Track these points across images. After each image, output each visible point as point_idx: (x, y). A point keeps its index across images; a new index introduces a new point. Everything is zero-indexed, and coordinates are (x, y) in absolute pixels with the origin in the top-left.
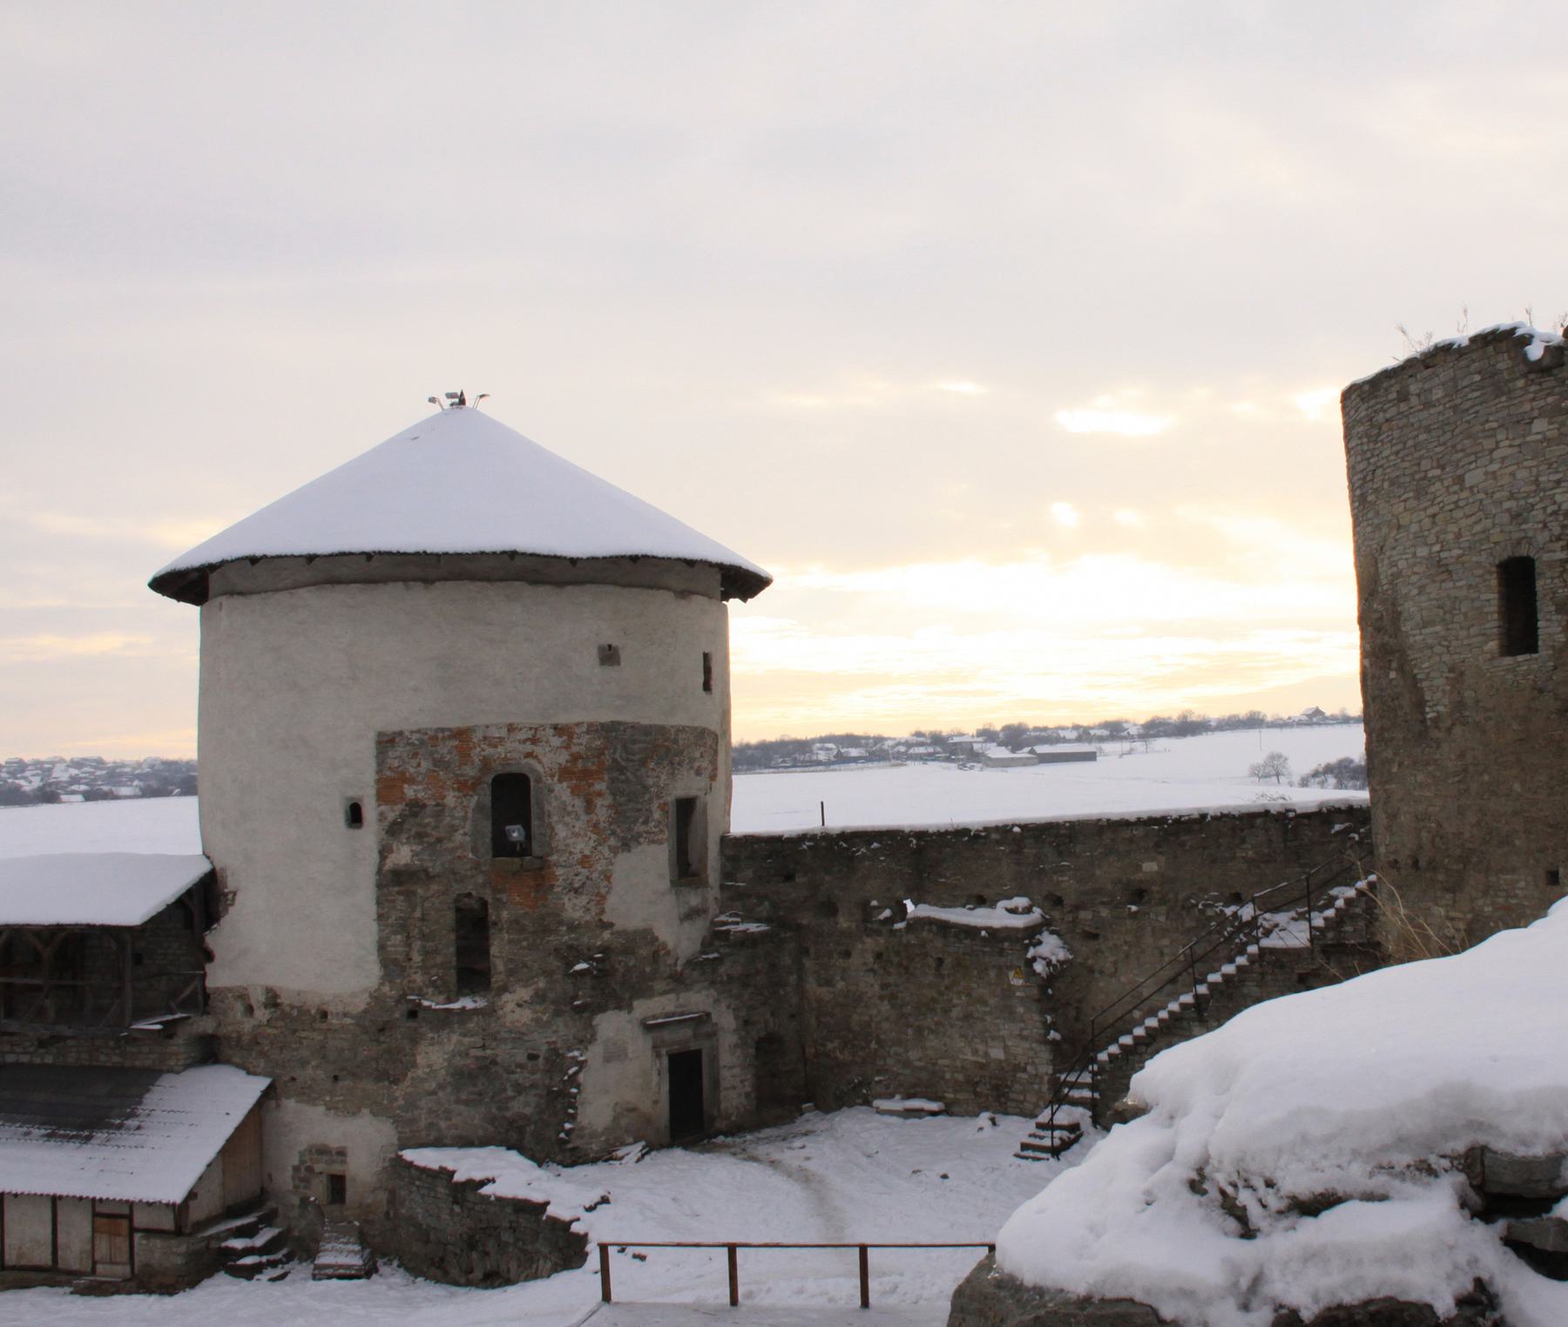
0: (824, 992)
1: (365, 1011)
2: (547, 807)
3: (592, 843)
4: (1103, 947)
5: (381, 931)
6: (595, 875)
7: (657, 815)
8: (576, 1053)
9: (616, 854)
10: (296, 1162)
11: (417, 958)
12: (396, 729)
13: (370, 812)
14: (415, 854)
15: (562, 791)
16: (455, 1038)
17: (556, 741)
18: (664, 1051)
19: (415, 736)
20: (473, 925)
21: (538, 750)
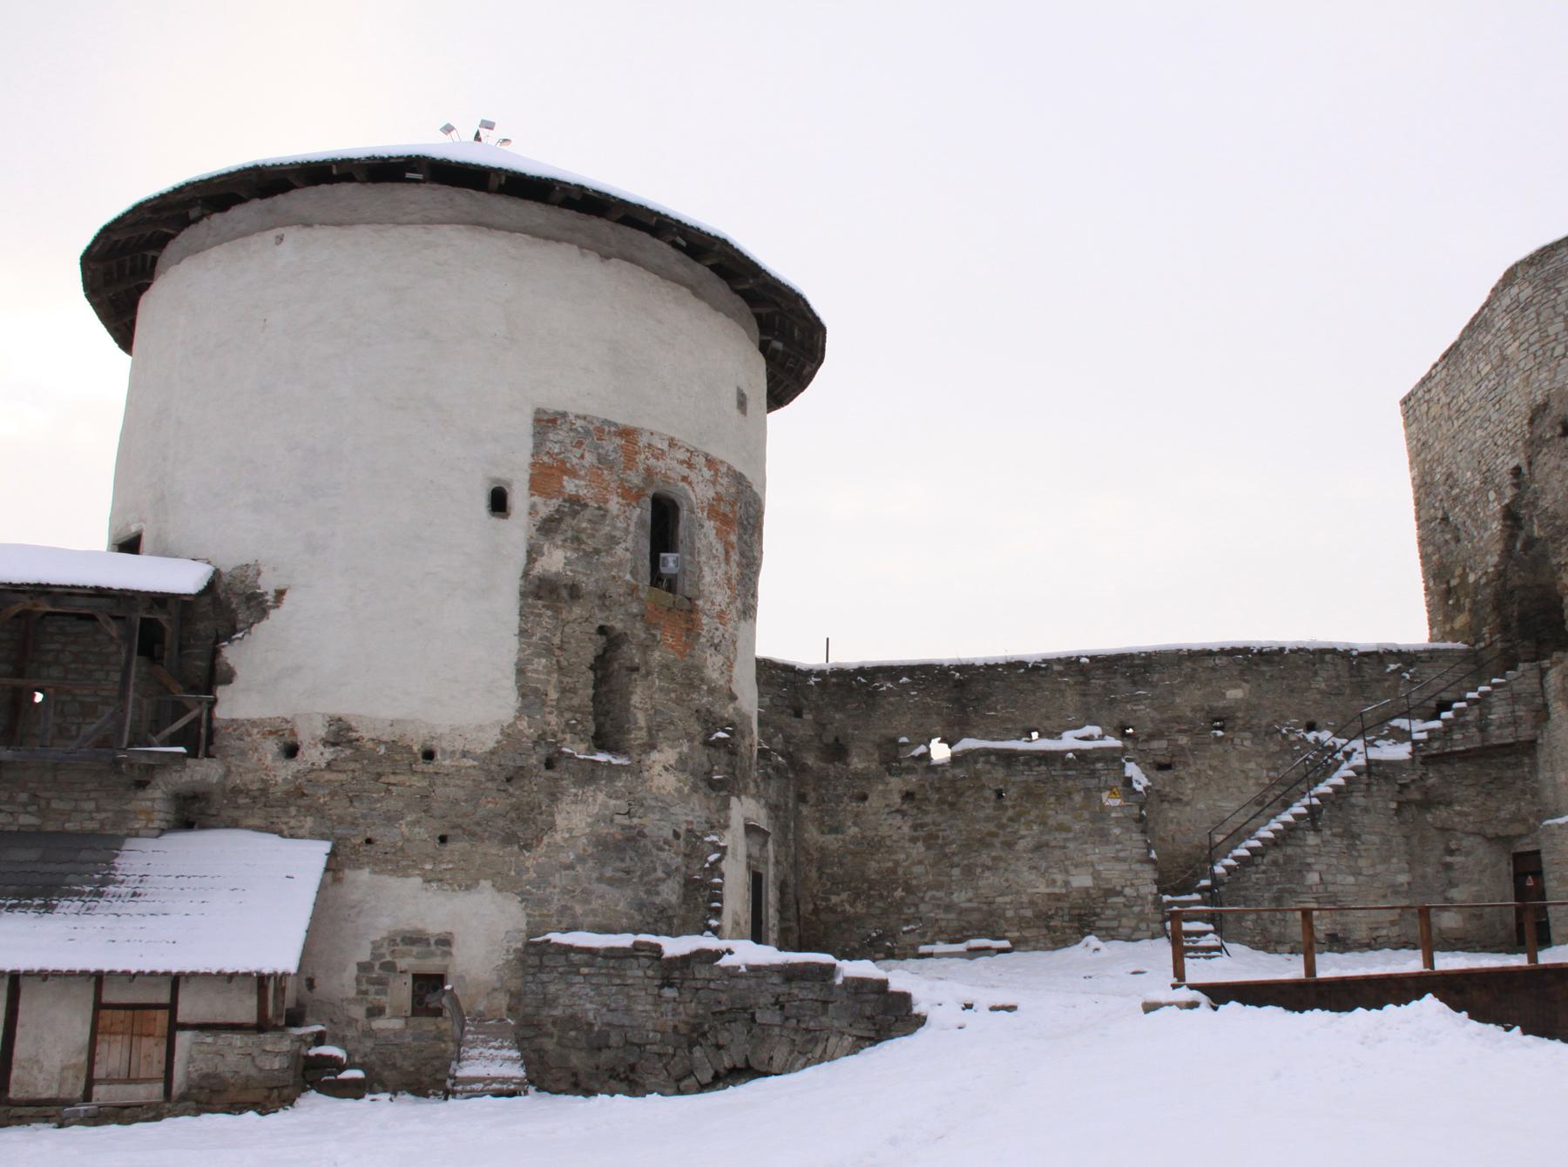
0: (831, 842)
1: (493, 752)
2: (698, 545)
4: (1183, 774)
5: (521, 650)
8: (714, 838)
10: (365, 956)
12: (561, 409)
13: (519, 499)
14: (568, 562)
16: (601, 797)
17: (707, 474)
19: (579, 423)
21: (693, 476)
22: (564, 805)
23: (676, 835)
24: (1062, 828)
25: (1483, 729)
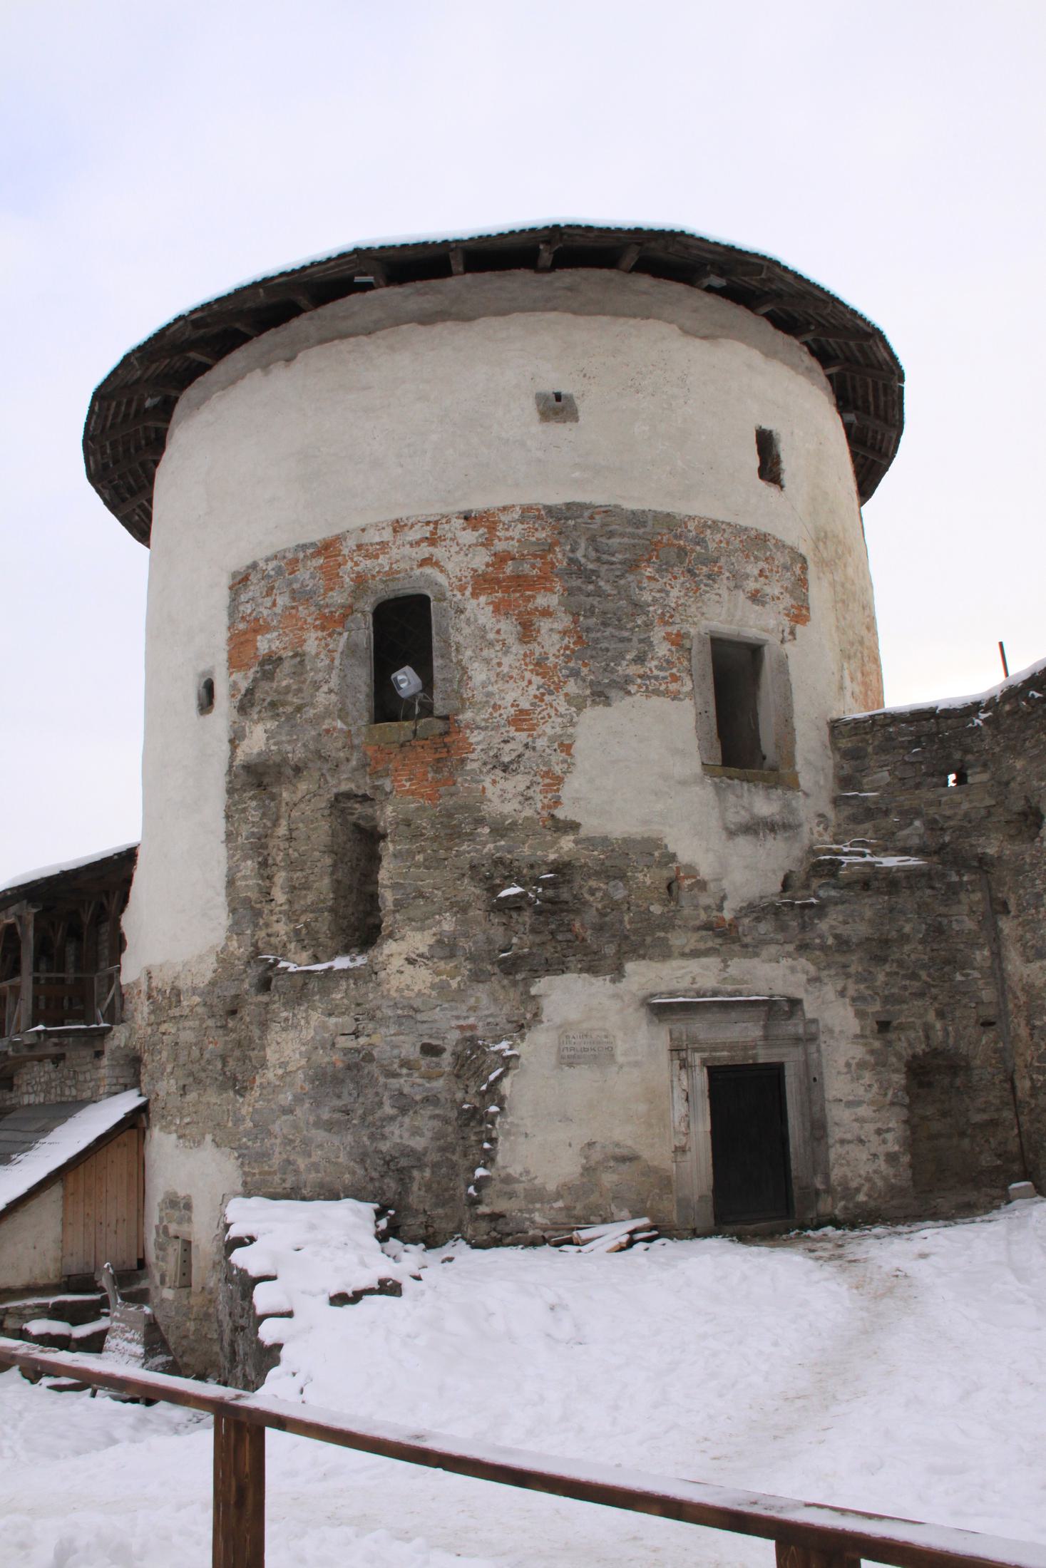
1: (213, 983)
2: (455, 637)
3: (533, 690)
5: (230, 857)
6: (541, 743)
7: (663, 649)
9: (580, 709)
11: (280, 896)
12: (249, 562)
14: (270, 735)
15: (480, 610)
16: (316, 1017)
17: (469, 537)
18: (696, 1058)
19: (272, 565)
20: (362, 845)
21: (439, 552)
22: (274, 1034)
23: (430, 1050)
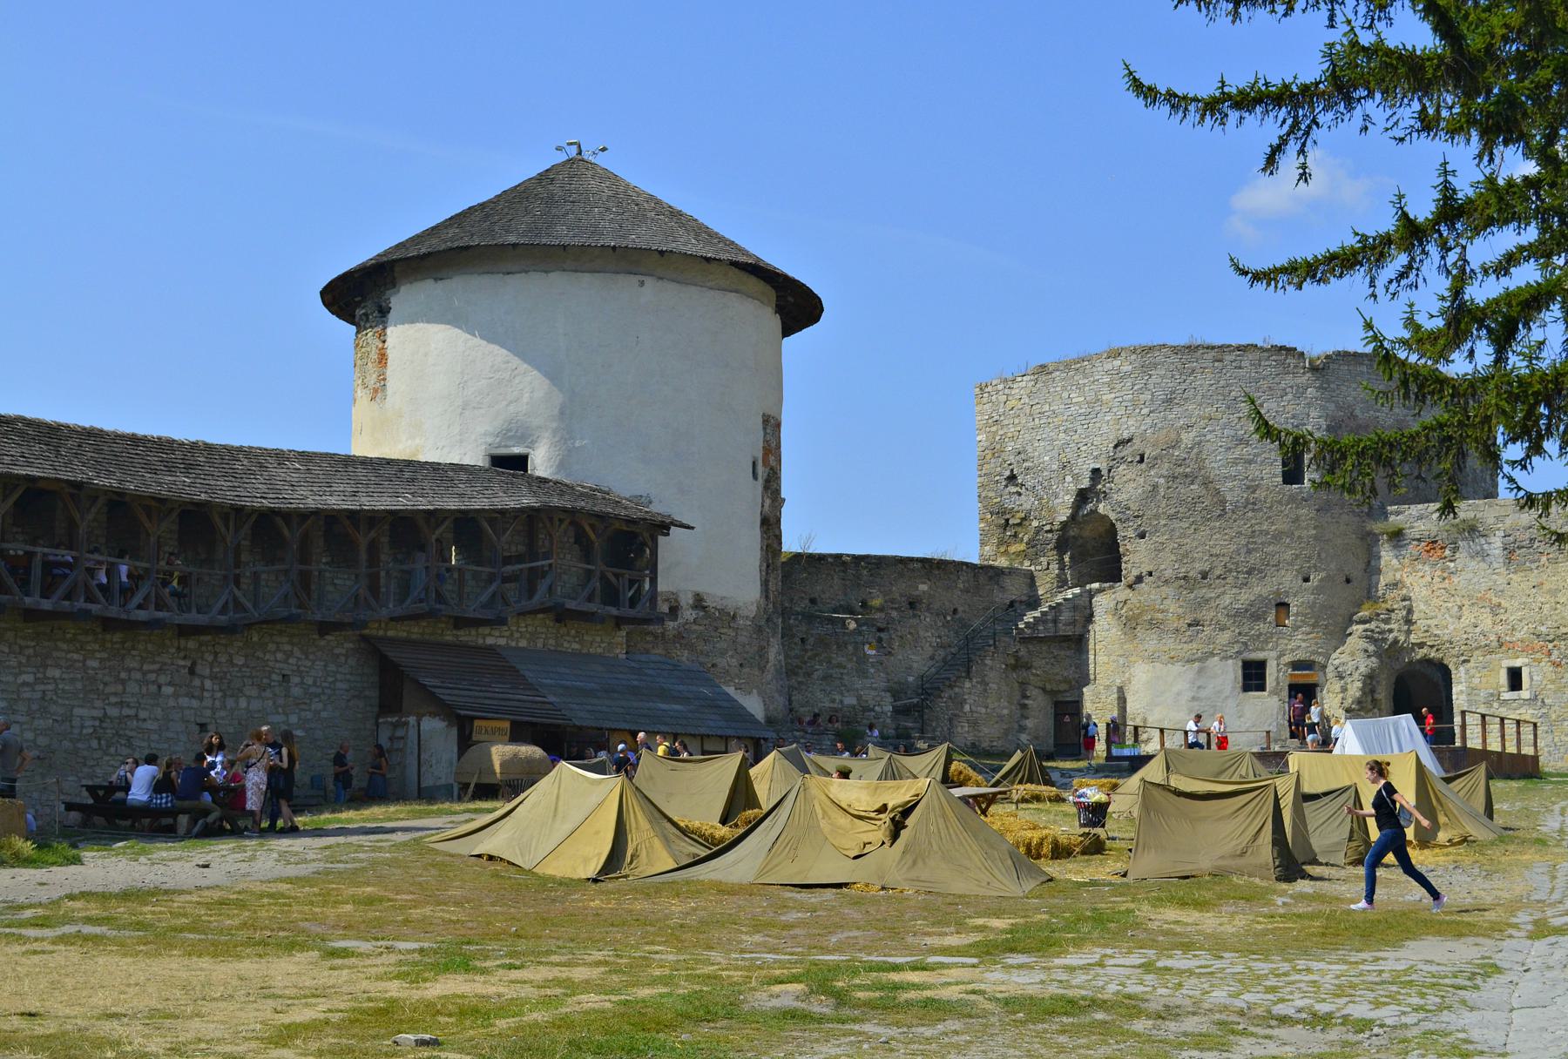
24: (840, 666)
25: (1055, 621)
